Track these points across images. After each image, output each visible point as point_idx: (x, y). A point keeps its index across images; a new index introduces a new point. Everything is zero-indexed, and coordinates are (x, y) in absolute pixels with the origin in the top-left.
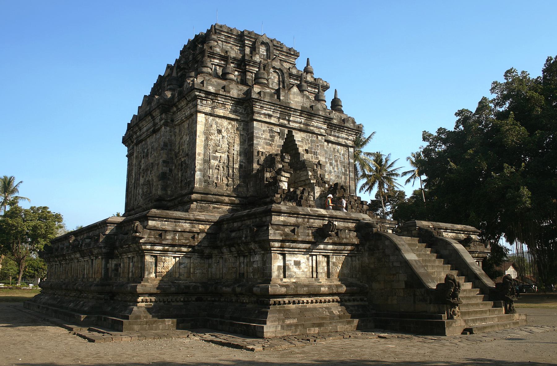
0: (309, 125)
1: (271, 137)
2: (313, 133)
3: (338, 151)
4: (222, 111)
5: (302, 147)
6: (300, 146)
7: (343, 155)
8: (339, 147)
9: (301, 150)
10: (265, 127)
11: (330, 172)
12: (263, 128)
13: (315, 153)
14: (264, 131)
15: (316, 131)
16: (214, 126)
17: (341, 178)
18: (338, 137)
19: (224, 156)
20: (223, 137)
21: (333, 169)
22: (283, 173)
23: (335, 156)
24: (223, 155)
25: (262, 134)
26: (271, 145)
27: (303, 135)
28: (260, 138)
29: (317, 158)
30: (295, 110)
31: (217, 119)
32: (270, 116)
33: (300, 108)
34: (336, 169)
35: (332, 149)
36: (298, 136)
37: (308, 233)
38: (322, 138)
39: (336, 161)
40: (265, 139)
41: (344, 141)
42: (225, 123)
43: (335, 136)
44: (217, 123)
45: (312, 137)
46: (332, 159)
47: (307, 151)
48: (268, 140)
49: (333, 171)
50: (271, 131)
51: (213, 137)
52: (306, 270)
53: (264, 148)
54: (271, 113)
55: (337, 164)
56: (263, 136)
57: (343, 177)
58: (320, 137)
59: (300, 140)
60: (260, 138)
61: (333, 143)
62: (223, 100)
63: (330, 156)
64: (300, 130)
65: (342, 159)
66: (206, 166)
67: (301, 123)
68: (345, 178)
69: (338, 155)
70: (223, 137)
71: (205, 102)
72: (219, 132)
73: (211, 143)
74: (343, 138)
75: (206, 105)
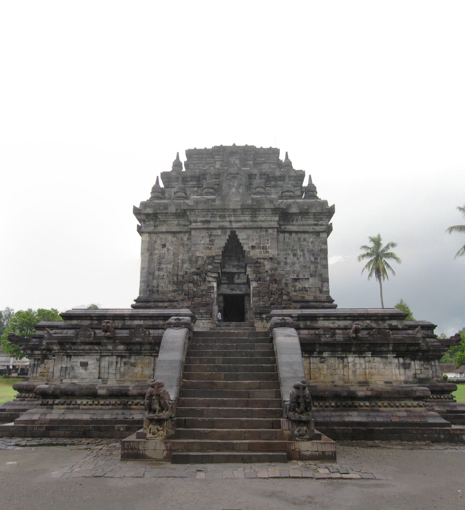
0: (256, 221)
1: (210, 241)
2: (261, 228)
3: (304, 240)
4: (165, 227)
5: (247, 244)
6: (246, 244)
7: (312, 242)
8: (306, 236)
9: (246, 248)
10: (204, 233)
11: (294, 264)
12: (202, 235)
13: (263, 248)
14: (203, 237)
15: (264, 225)
16: (159, 241)
17: (309, 268)
18: (303, 225)
19: (170, 266)
20: (168, 250)
21: (298, 259)
22: (209, 274)
23: (300, 245)
24: (169, 266)
25: (201, 241)
26: (210, 249)
27: (250, 232)
28: (198, 244)
29: (267, 252)
30: (234, 210)
31: (162, 236)
32: (208, 222)
33: (239, 207)
34: (302, 259)
35: (296, 239)
36: (242, 236)
37: (90, 335)
38: (274, 231)
39: (303, 251)
40: (203, 244)
41: (312, 227)
42: (170, 237)
43: (300, 225)
44: (161, 239)
45: (261, 231)
46: (296, 250)
47: (253, 247)
48: (208, 244)
49: (297, 261)
50: (210, 236)
51: (156, 252)
52: (94, 371)
53: (202, 253)
54: (208, 219)
55: (304, 254)
56: (202, 242)
57: (312, 267)
58: (270, 231)
59: (245, 237)
60: (198, 244)
61: (297, 232)
62: (164, 217)
63: (294, 247)
64: (245, 228)
65: (311, 246)
66: (151, 277)
67: (245, 221)
68: (316, 267)
69: (305, 243)
70: (168, 250)
71: (147, 223)
72: (164, 246)
73: (156, 257)
74: (310, 225)
75: (149, 226)
